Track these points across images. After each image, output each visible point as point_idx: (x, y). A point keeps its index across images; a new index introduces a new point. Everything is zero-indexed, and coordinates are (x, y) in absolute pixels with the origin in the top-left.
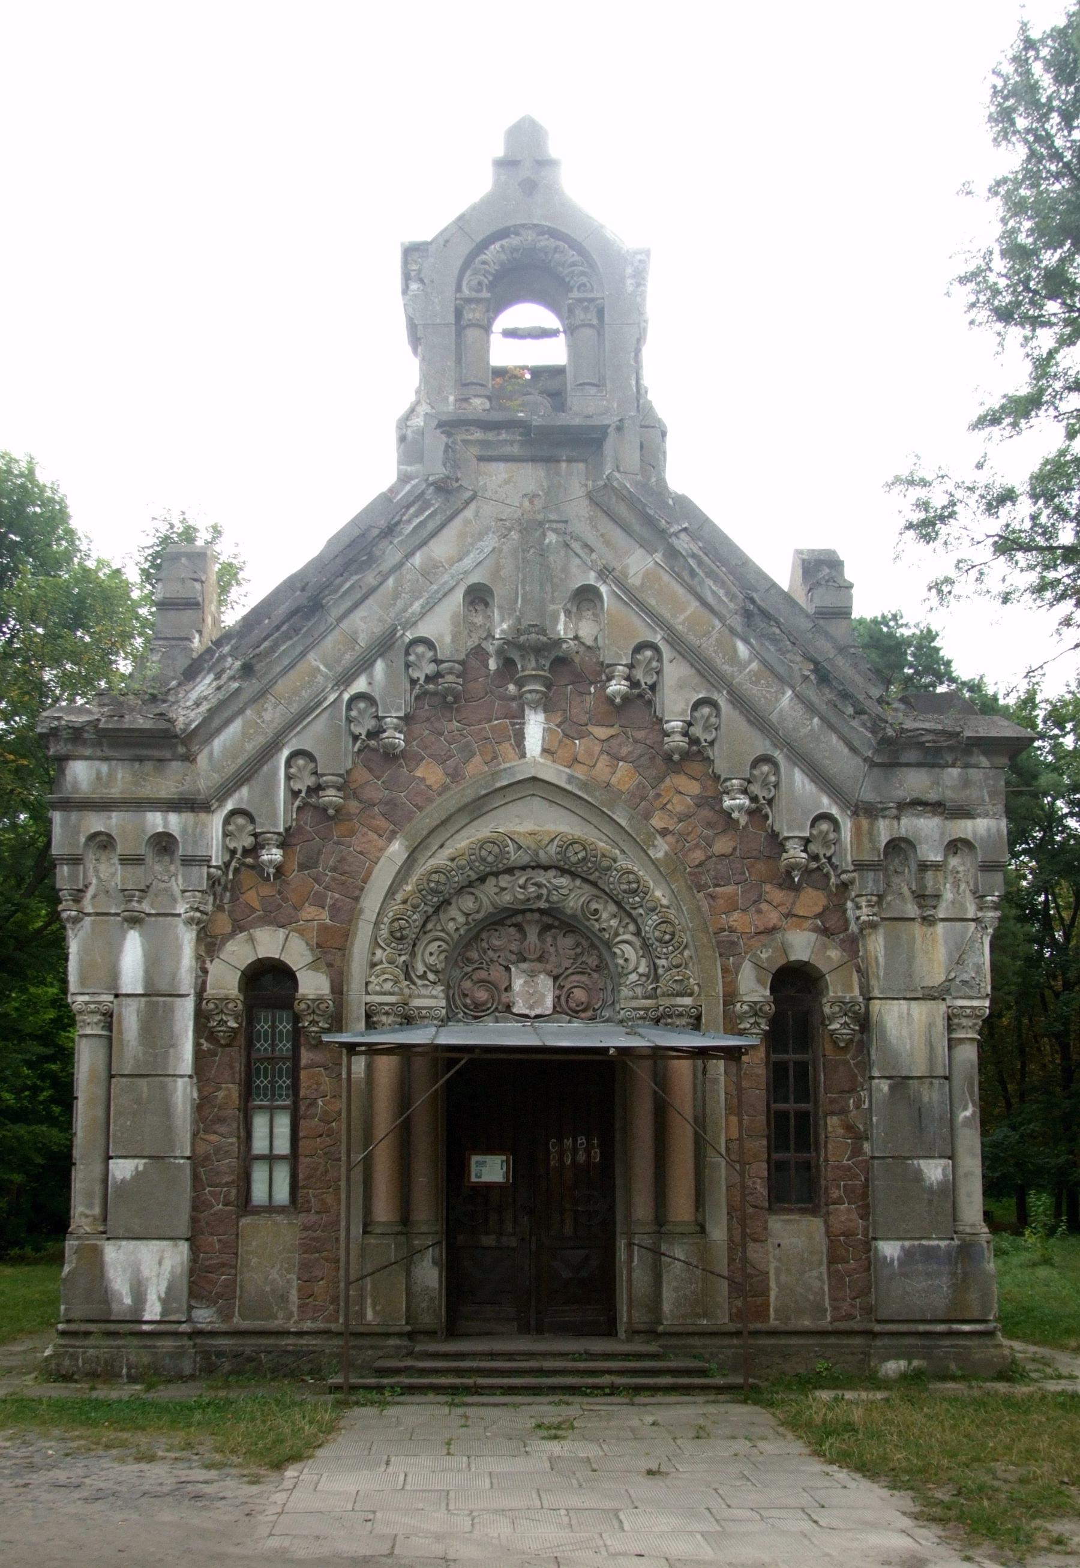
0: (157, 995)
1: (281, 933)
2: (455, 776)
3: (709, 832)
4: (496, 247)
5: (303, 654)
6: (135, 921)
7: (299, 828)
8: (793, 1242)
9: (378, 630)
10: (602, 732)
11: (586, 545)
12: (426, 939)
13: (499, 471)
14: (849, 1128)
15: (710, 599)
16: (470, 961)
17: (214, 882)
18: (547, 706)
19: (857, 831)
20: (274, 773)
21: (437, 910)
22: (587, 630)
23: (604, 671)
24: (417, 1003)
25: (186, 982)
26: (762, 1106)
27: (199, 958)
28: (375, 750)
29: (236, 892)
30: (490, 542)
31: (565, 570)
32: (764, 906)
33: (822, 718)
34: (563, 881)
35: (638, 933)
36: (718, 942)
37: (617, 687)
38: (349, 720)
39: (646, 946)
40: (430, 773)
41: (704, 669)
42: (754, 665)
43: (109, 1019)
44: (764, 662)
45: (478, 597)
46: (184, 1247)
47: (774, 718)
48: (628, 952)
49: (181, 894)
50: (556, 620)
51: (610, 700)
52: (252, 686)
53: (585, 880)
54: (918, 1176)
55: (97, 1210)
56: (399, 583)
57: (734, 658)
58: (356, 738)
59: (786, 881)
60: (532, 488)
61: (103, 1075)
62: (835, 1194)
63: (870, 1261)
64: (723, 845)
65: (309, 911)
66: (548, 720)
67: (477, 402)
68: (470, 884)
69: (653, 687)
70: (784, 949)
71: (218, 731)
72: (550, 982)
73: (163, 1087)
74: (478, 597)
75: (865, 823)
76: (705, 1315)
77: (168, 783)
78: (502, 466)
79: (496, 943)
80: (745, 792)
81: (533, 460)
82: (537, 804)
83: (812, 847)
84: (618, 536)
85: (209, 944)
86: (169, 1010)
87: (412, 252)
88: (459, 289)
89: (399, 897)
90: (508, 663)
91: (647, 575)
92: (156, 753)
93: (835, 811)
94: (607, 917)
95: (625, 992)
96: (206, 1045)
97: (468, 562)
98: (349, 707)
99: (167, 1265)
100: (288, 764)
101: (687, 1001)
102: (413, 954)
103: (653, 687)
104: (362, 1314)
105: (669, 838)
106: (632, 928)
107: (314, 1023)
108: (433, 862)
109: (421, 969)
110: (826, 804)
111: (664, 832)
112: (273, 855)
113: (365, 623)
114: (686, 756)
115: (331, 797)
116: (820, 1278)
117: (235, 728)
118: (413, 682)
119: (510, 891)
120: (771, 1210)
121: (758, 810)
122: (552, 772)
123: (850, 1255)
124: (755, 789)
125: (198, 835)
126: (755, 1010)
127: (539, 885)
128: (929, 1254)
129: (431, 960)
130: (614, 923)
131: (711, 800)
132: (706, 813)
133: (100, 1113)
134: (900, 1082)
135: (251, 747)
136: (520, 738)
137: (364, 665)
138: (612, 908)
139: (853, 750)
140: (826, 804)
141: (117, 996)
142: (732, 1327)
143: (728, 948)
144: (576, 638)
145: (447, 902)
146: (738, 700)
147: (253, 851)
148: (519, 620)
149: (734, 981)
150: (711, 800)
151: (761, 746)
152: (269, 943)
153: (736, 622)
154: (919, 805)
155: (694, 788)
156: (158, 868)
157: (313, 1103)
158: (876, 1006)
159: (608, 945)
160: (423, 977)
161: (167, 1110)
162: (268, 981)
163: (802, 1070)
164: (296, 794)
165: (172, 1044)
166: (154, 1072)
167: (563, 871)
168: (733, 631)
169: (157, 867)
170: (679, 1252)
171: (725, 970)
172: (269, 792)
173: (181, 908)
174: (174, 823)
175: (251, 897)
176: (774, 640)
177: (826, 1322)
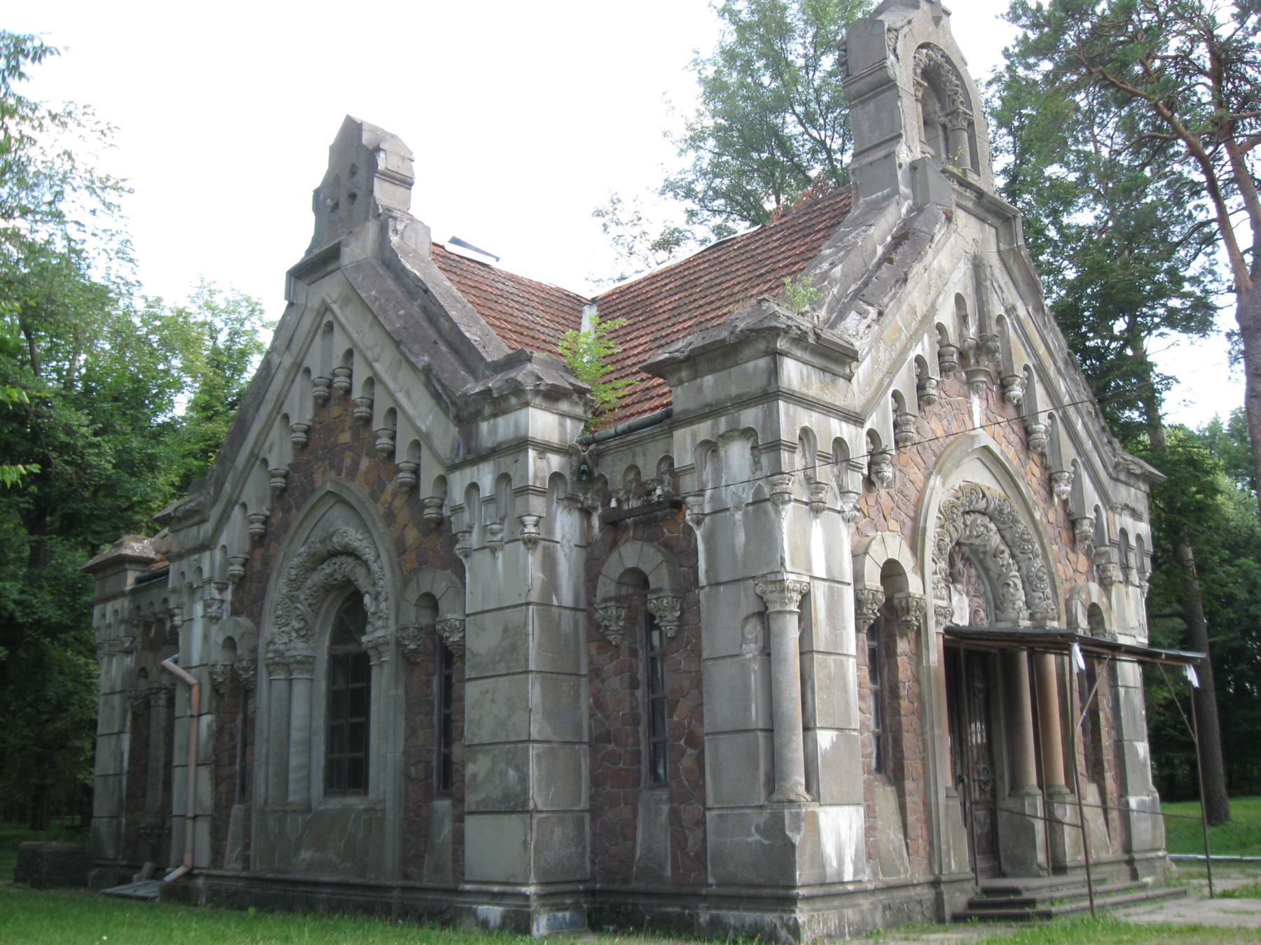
11: (1000, 287)
43: (806, 597)
46: (861, 810)
56: (929, 276)
86: (841, 596)
99: (854, 831)
136: (970, 412)
141: (812, 577)
153: (1061, 364)
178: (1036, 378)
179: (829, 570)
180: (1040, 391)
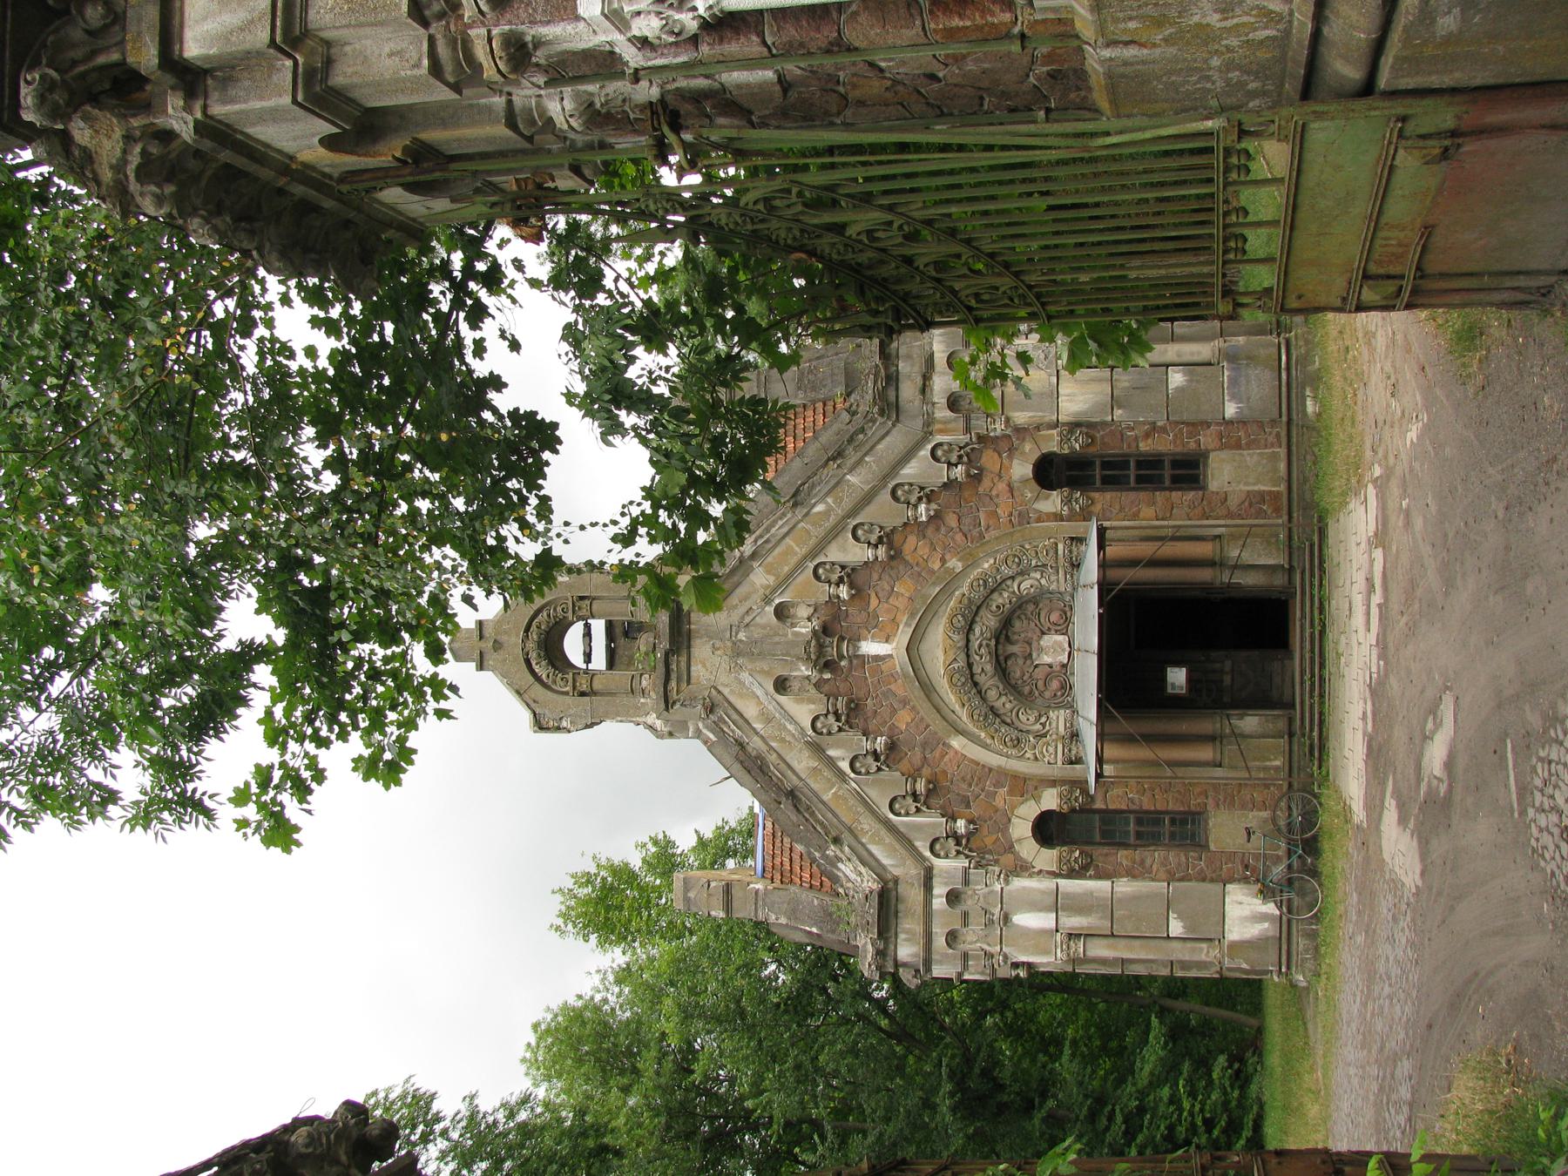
0: (1057, 904)
1: (1014, 820)
2: (905, 702)
3: (943, 529)
4: (537, 669)
5: (824, 803)
6: (1006, 918)
7: (942, 808)
8: (1228, 474)
9: (806, 753)
10: (874, 602)
12: (1017, 723)
13: (696, 669)
14: (1147, 435)
15: (785, 530)
16: (1031, 692)
17: (978, 866)
18: (855, 640)
19: (941, 431)
20: (906, 824)
21: (997, 715)
22: (803, 612)
23: (834, 601)
24: (1061, 729)
25: (1048, 884)
26: (1132, 495)
27: (1030, 876)
28: (887, 757)
29: (981, 845)
30: (745, 676)
31: (763, 627)
32: (994, 493)
33: (866, 454)
34: (977, 631)
35: (1013, 578)
36: (1020, 524)
37: (844, 591)
38: (868, 773)
39: (1022, 573)
40: (903, 719)
41: (833, 534)
42: (829, 500)
44: (827, 494)
45: (781, 685)
47: (867, 488)
48: (1026, 585)
49: (987, 886)
50: (797, 634)
51: (852, 597)
52: (846, 836)
53: (976, 613)
54: (1180, 390)
55: (1204, 945)
56: (775, 738)
57: (827, 513)
58: (879, 769)
59: (977, 478)
60: (708, 648)
61: (1111, 940)
62: (1192, 445)
63: (1239, 422)
64: (951, 520)
65: (999, 802)
66: (866, 639)
67: (644, 683)
68: (979, 692)
69: (843, 567)
70: (1025, 481)
71: (877, 860)
72: (1046, 637)
73: (1120, 900)
74: (781, 685)
75: (937, 426)
76: (1277, 536)
77: (912, 895)
78: (693, 668)
79: (1018, 674)
80: (916, 506)
81: (689, 647)
82: (924, 647)
83: (954, 459)
84: (740, 591)
85: (1022, 868)
86: (1068, 895)
87: (540, 726)
88: (567, 693)
89: (989, 741)
90: (828, 665)
91: (768, 572)
92: (893, 902)
93: (929, 447)
94: (1002, 599)
95: (1053, 587)
96: (1091, 872)
97: (759, 692)
98: (859, 773)
99: (1240, 898)
100: (898, 815)
101: (1060, 547)
102: (1028, 732)
103: (843, 567)
104: (1277, 769)
105: (947, 557)
106: (1009, 582)
107: (1076, 799)
108: (964, 718)
109: (1038, 727)
110: (925, 452)
111: (943, 561)
112: (961, 825)
113: (802, 762)
114: (891, 546)
115: (921, 786)
116: (1251, 456)
117: (874, 849)
118: (840, 730)
119: (984, 664)
120: (1204, 488)
121: (927, 496)
122: (903, 636)
123: (1234, 435)
124: (913, 500)
125: (948, 873)
126: (1067, 501)
127: (980, 646)
128: (1234, 382)
129: (1032, 719)
130: (1006, 595)
131: (920, 528)
132: (930, 532)
133: (1137, 943)
134: (1114, 402)
135: (888, 838)
136: (877, 658)
137: (831, 763)
138: (995, 595)
139: (887, 433)
140: (925, 452)
142: (1285, 518)
143: (1024, 518)
144: (809, 619)
145: (992, 708)
146: (853, 512)
147: (958, 840)
148: (799, 659)
149: (1048, 514)
150: (920, 528)
151: (885, 496)
152: (1021, 829)
153: (800, 512)
154: (924, 390)
155: (912, 540)
156: (969, 902)
157: (1132, 800)
158: (1062, 418)
159: (1020, 597)
160: (1044, 725)
161: (1135, 898)
162: (1047, 829)
163: (1106, 465)
164: (918, 810)
165: (1089, 894)
166: (1110, 907)
167: (970, 629)
168: (807, 514)
169: (969, 904)
170: (1235, 553)
171: (1039, 520)
172: (919, 828)
173: (998, 887)
174: (940, 891)
175: (989, 841)
176: (813, 486)
177: (1282, 451)
178: (821, 559)
179: (1046, 909)
180: (834, 554)
